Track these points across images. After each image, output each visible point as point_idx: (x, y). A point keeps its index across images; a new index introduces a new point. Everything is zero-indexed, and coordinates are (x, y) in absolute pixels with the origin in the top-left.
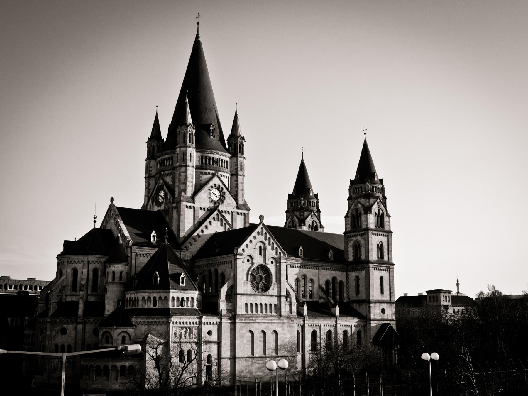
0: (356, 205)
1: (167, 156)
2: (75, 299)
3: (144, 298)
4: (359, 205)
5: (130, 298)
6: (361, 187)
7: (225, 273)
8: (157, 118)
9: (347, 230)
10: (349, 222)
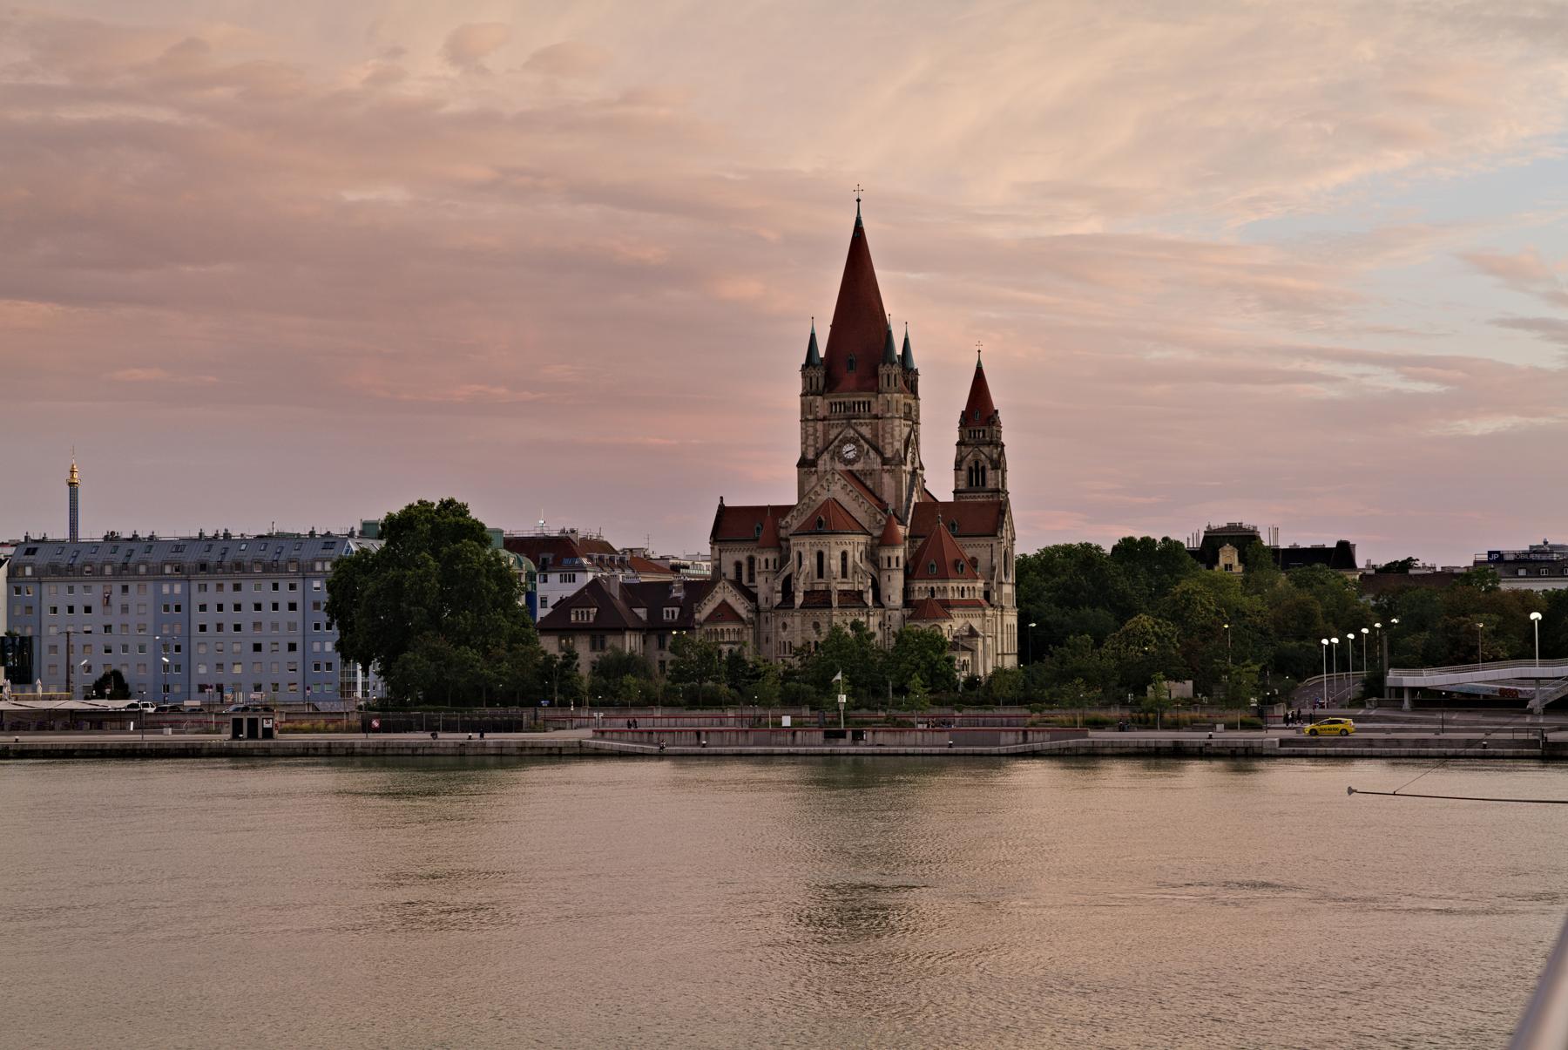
0: (974, 455)
1: (861, 399)
2: (846, 587)
3: (952, 587)
4: (983, 456)
5: (926, 588)
6: (984, 431)
7: (978, 558)
8: (813, 336)
9: (960, 488)
10: (964, 477)
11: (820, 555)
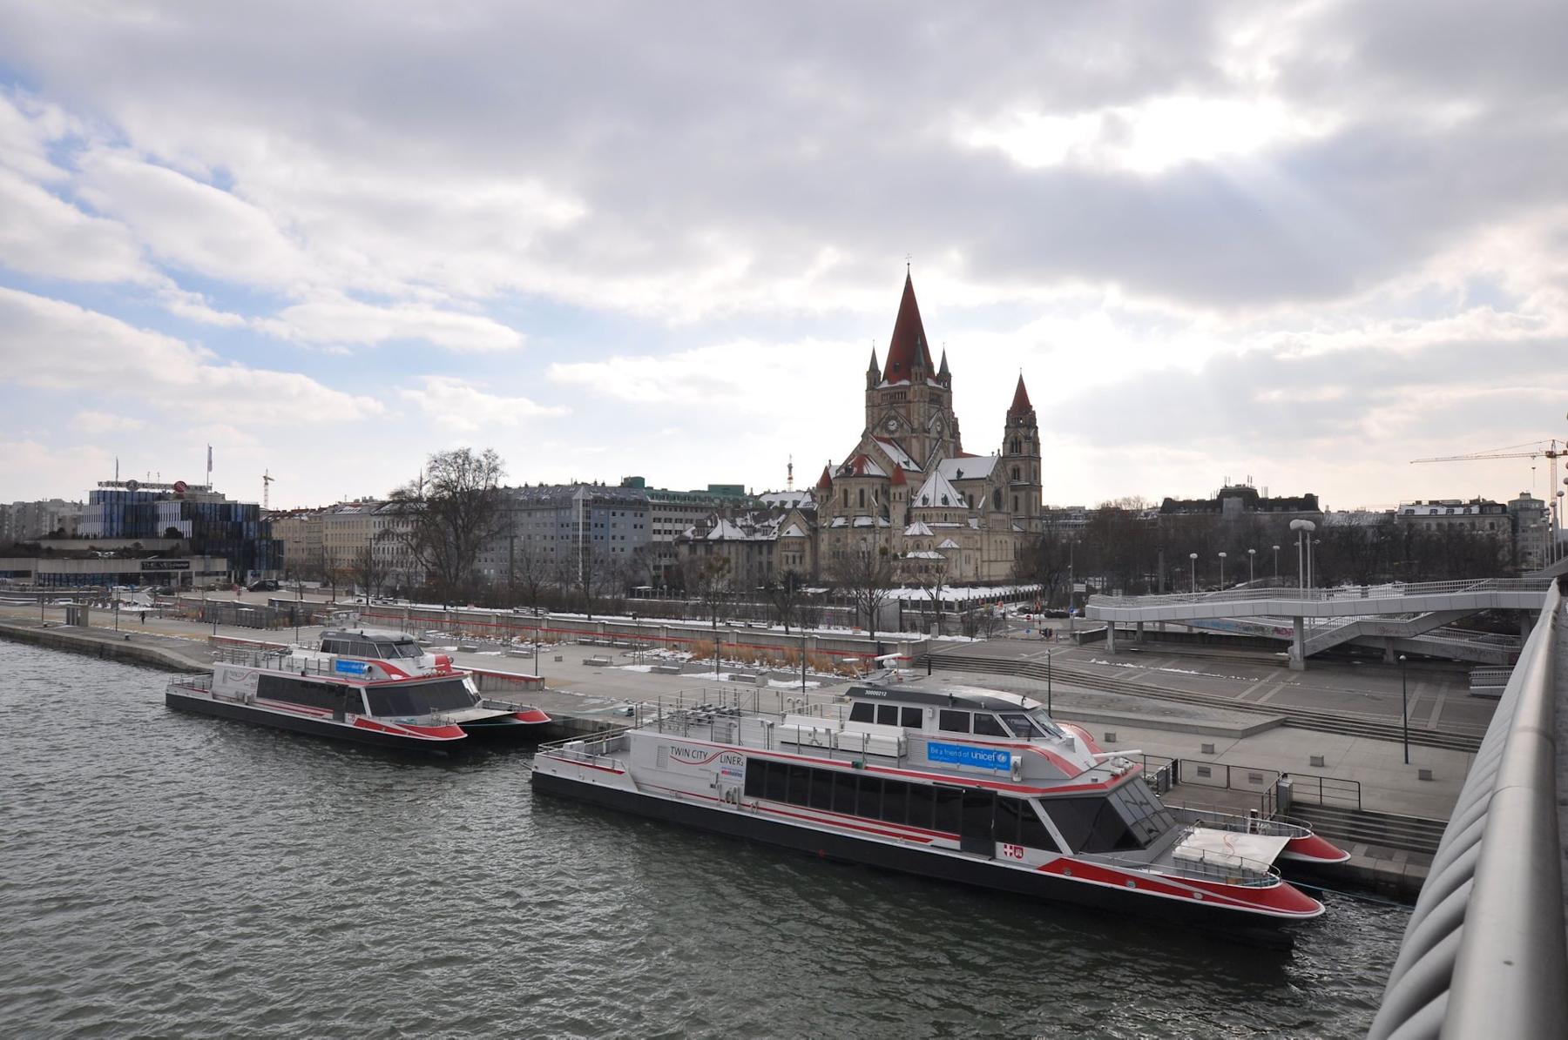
11: (846, 492)
